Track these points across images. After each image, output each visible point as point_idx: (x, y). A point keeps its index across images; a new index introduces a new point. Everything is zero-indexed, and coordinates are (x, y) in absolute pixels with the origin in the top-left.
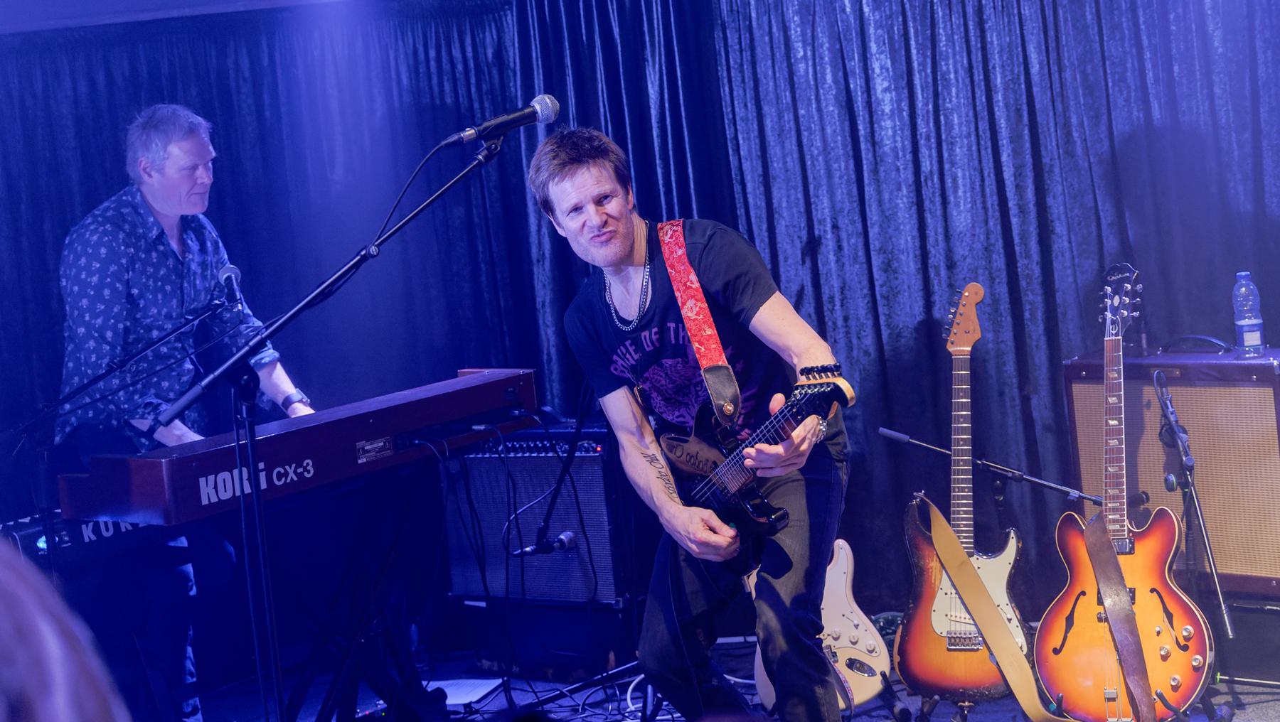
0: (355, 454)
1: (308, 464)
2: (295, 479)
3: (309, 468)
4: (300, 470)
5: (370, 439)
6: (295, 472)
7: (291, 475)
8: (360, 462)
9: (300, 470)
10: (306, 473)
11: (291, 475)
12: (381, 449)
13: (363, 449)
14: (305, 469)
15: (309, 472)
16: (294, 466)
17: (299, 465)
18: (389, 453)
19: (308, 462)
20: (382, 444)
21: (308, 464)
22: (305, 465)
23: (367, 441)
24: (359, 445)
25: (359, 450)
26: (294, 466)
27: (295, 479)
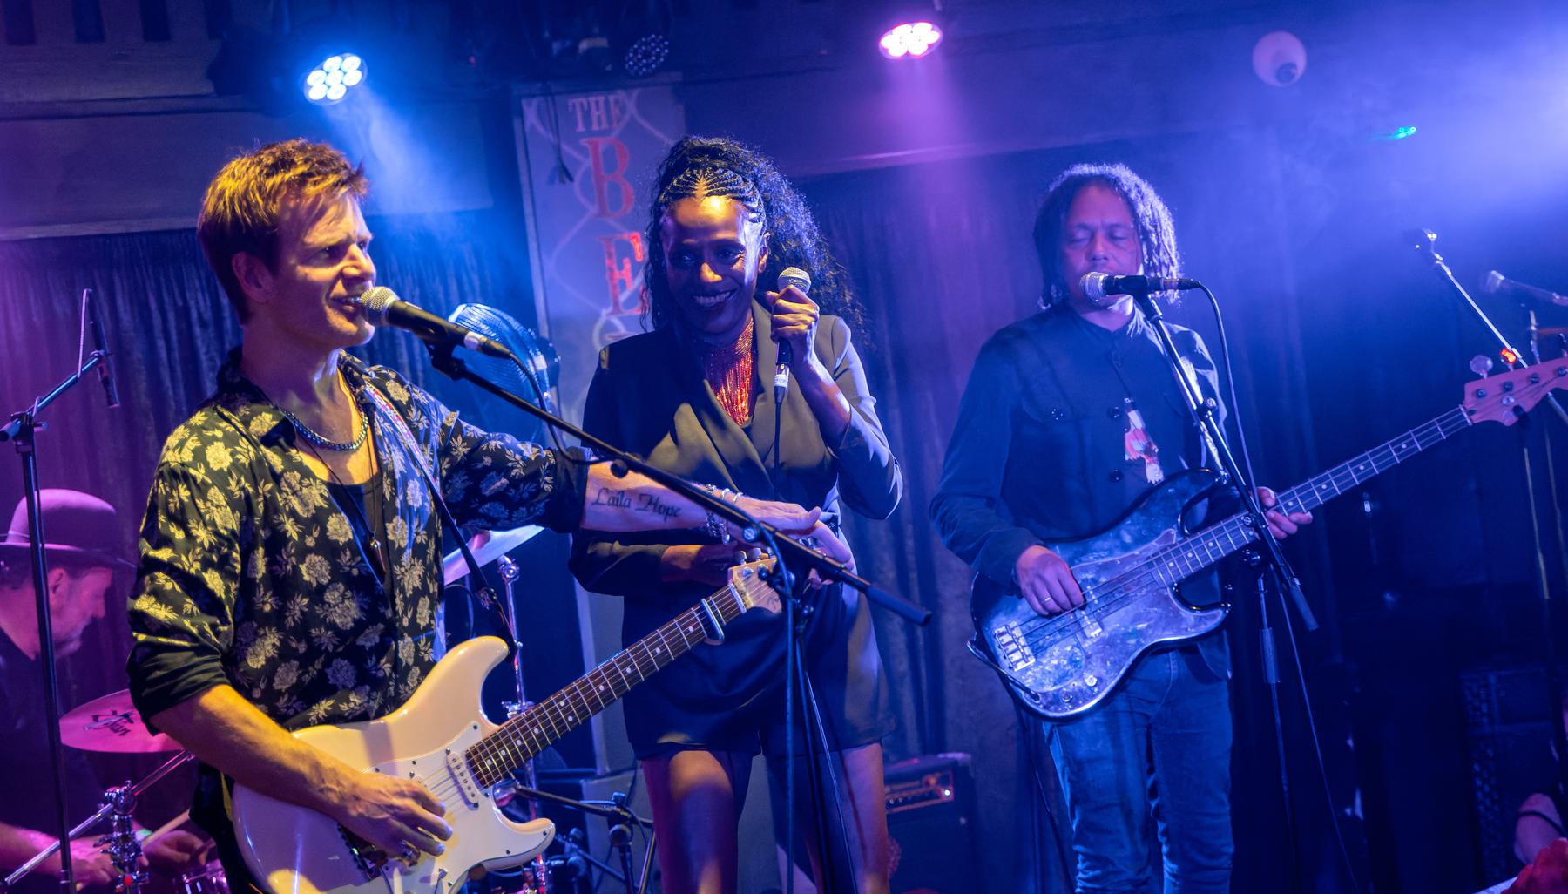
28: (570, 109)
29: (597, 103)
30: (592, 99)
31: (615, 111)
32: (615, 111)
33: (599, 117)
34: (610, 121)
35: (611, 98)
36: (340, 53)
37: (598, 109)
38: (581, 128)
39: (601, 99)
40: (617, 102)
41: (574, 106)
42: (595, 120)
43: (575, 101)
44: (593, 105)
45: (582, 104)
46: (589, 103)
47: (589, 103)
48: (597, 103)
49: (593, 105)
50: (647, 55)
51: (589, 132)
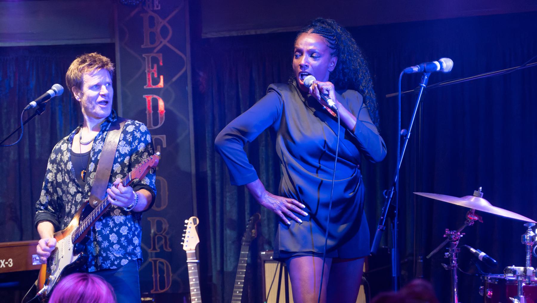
1: (10, 261)
2: (4, 266)
3: (11, 262)
4: (7, 263)
6: (4, 263)
8: (34, 264)
9: (7, 263)
10: (9, 265)
13: (36, 258)
14: (9, 263)
15: (10, 264)
16: (4, 260)
17: (6, 261)
19: (11, 260)
21: (10, 261)
22: (9, 261)
25: (34, 258)
26: (4, 260)
27: (4, 266)
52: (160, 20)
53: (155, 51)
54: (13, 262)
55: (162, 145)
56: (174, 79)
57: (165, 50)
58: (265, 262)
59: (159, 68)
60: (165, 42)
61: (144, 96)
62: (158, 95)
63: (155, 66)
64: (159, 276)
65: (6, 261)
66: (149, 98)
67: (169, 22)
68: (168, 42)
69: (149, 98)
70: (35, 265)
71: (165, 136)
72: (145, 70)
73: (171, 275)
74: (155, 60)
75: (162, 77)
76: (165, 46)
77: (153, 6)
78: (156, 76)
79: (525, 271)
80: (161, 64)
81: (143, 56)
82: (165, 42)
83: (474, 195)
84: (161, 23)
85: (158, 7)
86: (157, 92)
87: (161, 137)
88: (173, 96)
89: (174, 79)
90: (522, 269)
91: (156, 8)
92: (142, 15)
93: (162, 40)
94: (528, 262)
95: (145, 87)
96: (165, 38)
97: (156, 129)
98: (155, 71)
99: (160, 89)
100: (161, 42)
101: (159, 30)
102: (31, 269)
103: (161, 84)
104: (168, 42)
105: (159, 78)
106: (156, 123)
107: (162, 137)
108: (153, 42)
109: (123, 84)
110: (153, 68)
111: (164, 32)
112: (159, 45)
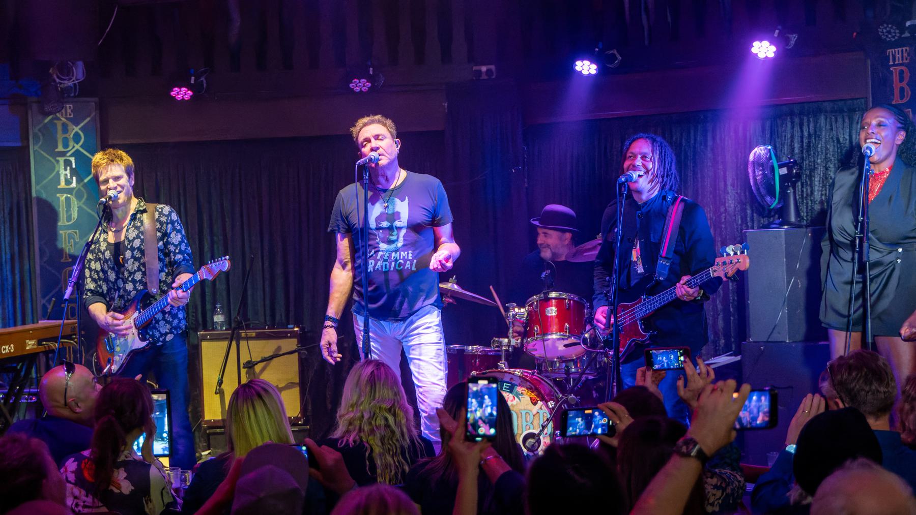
0: (25, 345)
3: (12, 348)
5: (31, 339)
7: (7, 350)
8: (28, 348)
9: (10, 348)
11: (7, 350)
12: (34, 345)
14: (11, 349)
16: (8, 346)
18: (35, 347)
19: (12, 345)
20: (33, 342)
23: (30, 340)
24: (27, 341)
28: (888, 54)
29: (898, 51)
30: (896, 50)
31: (905, 55)
32: (905, 55)
33: (899, 57)
34: (903, 60)
35: (904, 49)
36: (761, 40)
37: (898, 54)
38: (891, 63)
39: (900, 49)
40: (906, 50)
41: (889, 52)
42: (897, 59)
43: (890, 50)
44: (897, 53)
45: (892, 51)
46: (895, 51)
47: (895, 51)
48: (898, 51)
49: (897, 53)
50: (889, 32)
51: (894, 65)
52: (74, 127)
53: (68, 154)
54: (14, 347)
55: (74, 239)
56: (86, 181)
57: (77, 154)
58: (201, 342)
59: (71, 168)
60: (77, 147)
61: (58, 195)
62: (71, 194)
63: (68, 168)
64: (72, 356)
65: (9, 347)
66: (63, 198)
67: (80, 129)
68: (81, 146)
69: (63, 198)
70: (28, 350)
71: (78, 231)
72: (58, 172)
73: (84, 355)
74: (67, 163)
75: (74, 178)
76: (77, 150)
77: (66, 114)
78: (69, 177)
79: (509, 342)
80: (74, 166)
81: (58, 158)
82: (77, 147)
83: (450, 281)
84: (74, 129)
85: (70, 115)
86: (70, 191)
87: (74, 232)
88: (85, 196)
89: (86, 181)
90: (506, 340)
91: (68, 116)
92: (56, 121)
93: (75, 145)
94: (511, 335)
95: (59, 187)
96: (77, 144)
97: (68, 225)
98: (68, 172)
99: (73, 189)
100: (74, 147)
101: (72, 136)
102: (25, 353)
103: (74, 185)
104: (81, 146)
105: (71, 177)
106: (69, 218)
107: (76, 233)
108: (66, 145)
109: (37, 183)
110: (66, 170)
111: (77, 138)
112: (72, 149)
